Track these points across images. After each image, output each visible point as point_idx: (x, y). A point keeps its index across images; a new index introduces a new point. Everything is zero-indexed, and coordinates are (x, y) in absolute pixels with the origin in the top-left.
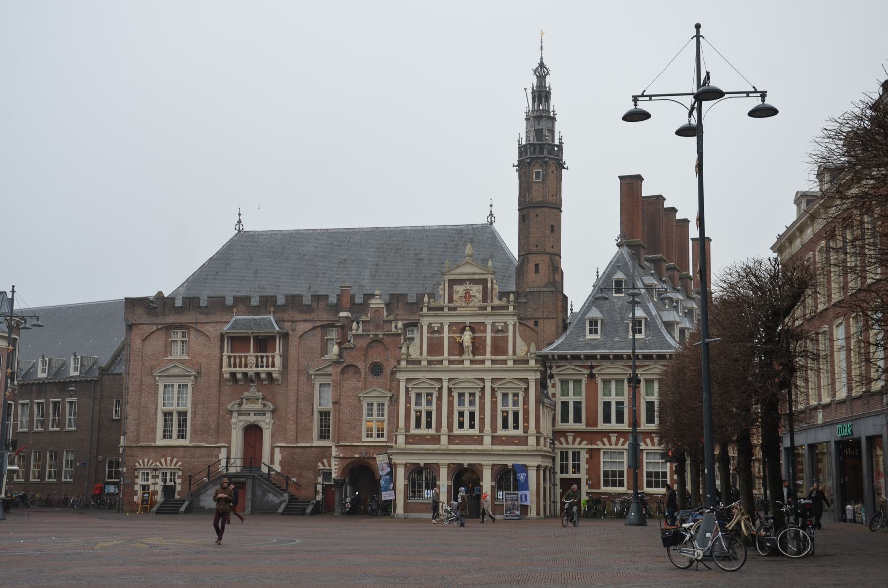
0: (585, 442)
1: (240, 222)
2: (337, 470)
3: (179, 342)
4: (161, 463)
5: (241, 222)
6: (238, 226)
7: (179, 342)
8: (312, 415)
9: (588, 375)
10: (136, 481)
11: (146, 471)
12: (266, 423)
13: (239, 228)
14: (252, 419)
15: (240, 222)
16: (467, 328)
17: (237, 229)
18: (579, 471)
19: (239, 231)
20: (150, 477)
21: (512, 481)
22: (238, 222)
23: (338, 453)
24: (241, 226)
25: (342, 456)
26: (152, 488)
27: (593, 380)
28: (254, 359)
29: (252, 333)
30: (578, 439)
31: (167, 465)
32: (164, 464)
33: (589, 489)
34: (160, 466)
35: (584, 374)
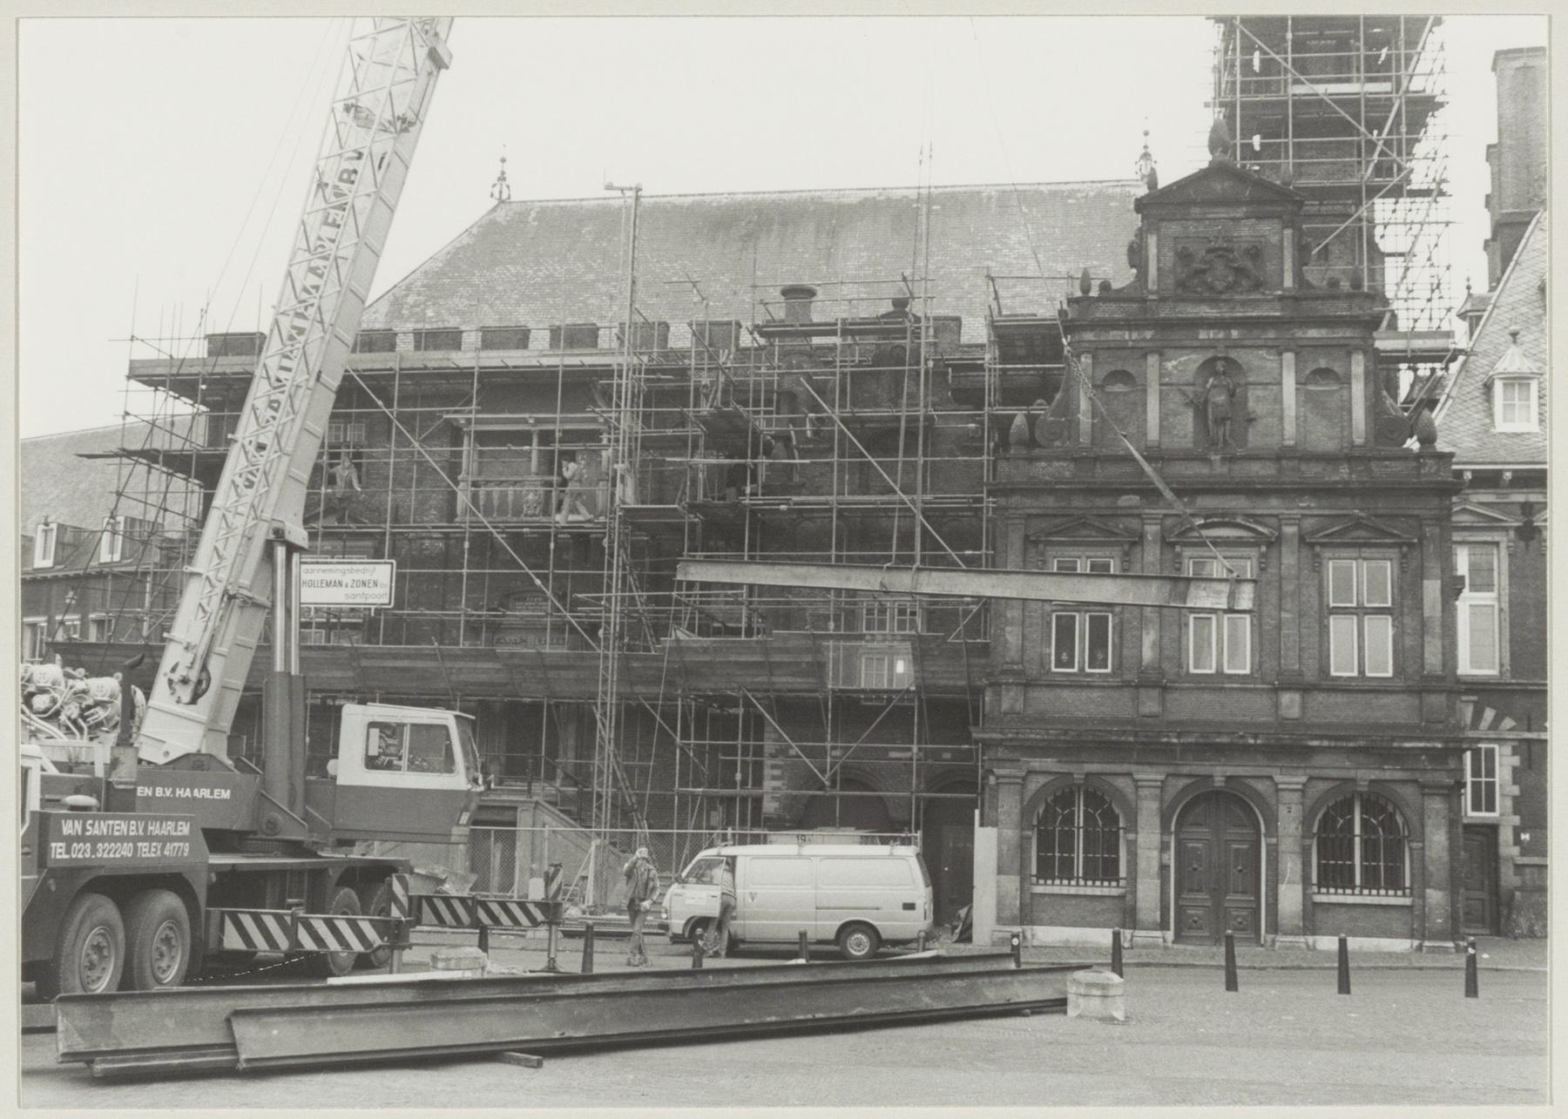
0: (1508, 723)
1: (502, 178)
5: (504, 179)
6: (496, 191)
9: (1517, 529)
13: (501, 192)
15: (502, 178)
16: (1220, 366)
17: (497, 195)
18: (1491, 807)
19: (501, 201)
21: (1357, 830)
22: (499, 179)
24: (505, 189)
27: (1533, 544)
30: (1489, 714)
33: (1523, 854)
35: (1506, 529)
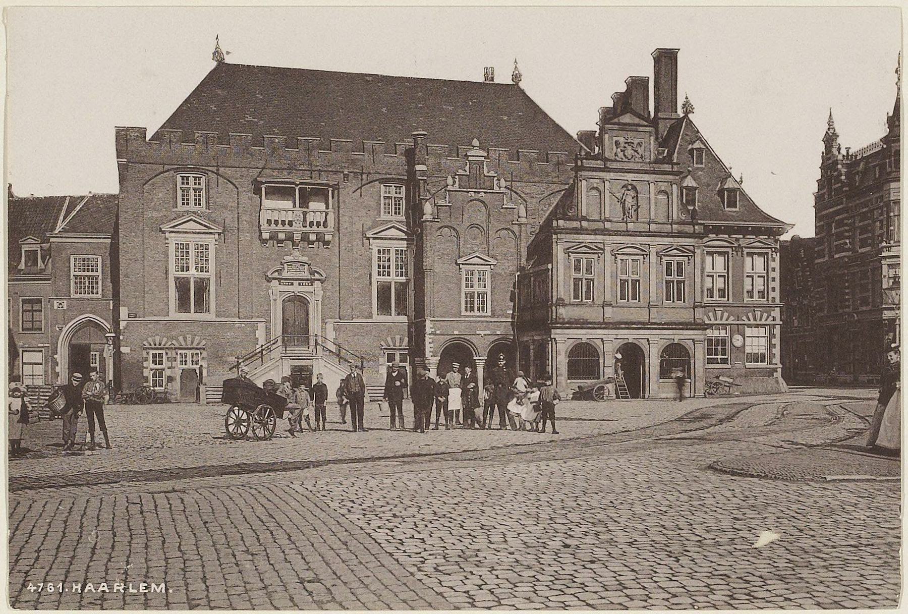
2: (432, 350)
3: (192, 189)
4: (177, 340)
7: (192, 189)
8: (371, 284)
10: (145, 364)
11: (157, 352)
12: (315, 294)
14: (296, 288)
20: (165, 359)
23: (433, 330)
25: (438, 332)
26: (168, 373)
28: (302, 216)
29: (301, 183)
31: (186, 345)
32: (183, 343)
34: (177, 346)
